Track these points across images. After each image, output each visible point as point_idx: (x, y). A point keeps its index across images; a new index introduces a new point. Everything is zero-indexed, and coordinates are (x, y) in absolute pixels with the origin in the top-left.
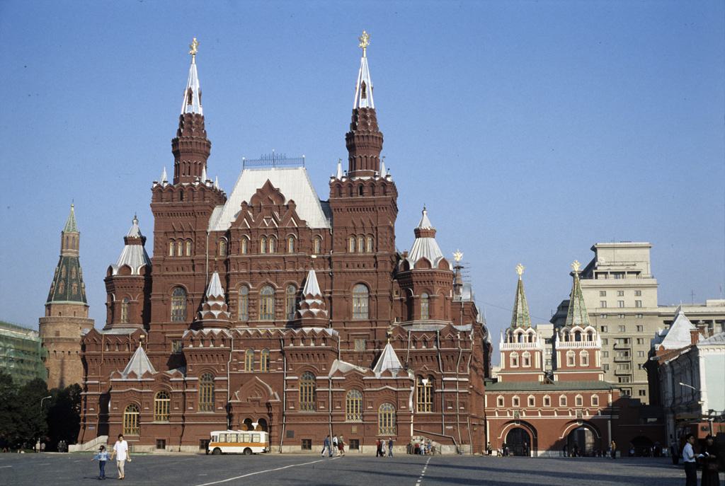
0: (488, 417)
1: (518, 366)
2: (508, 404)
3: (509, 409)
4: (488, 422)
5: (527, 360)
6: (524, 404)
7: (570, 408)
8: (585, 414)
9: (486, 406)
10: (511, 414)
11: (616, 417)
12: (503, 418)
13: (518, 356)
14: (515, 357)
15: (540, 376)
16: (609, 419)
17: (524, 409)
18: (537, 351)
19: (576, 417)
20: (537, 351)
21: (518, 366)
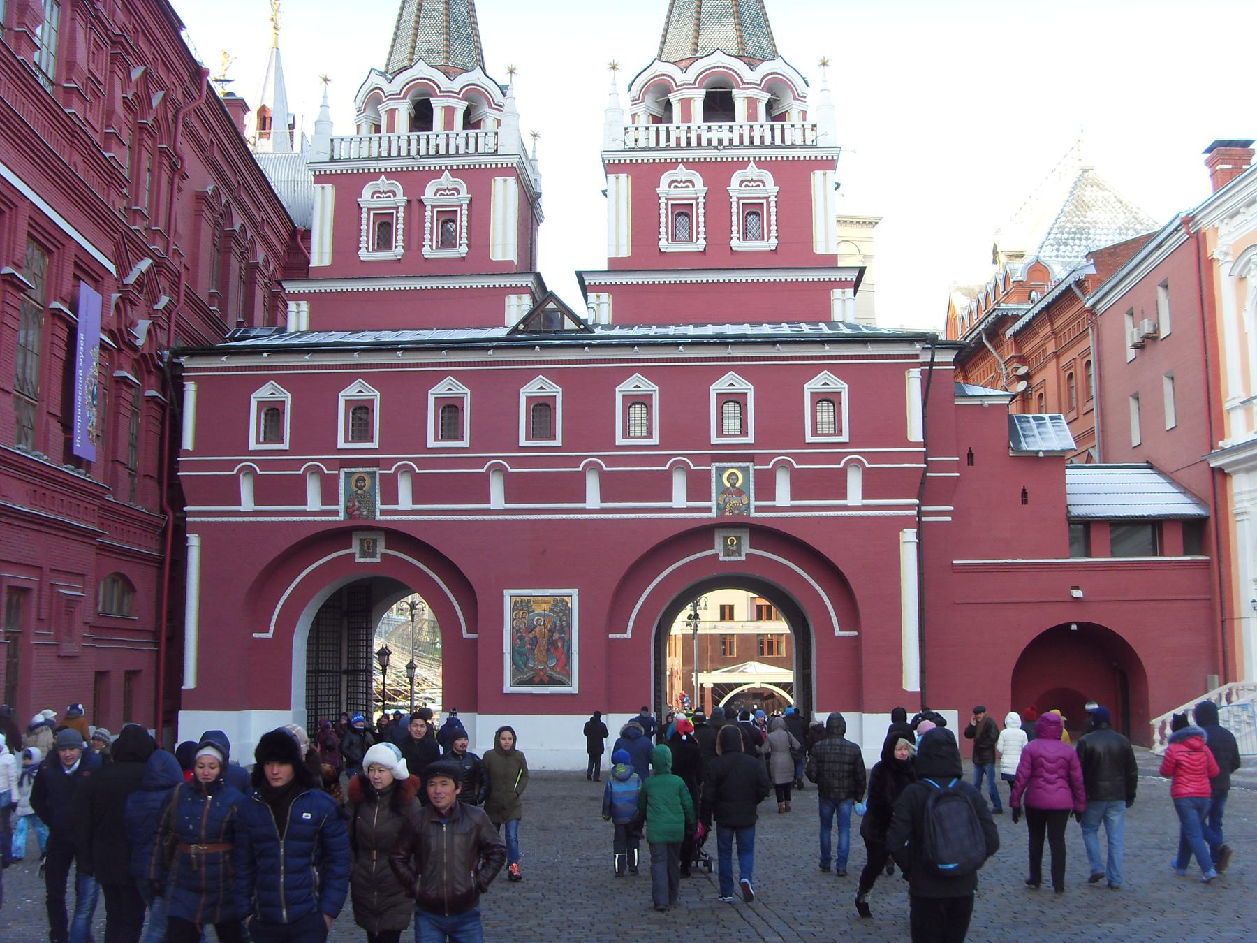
1: (398, 251)
2: (316, 433)
3: (314, 459)
4: (194, 540)
6: (404, 432)
7: (680, 455)
8: (766, 487)
9: (188, 442)
10: (329, 494)
11: (940, 513)
12: (280, 513)
13: (401, 199)
14: (385, 203)
15: (512, 300)
16: (905, 522)
17: (407, 458)
19: (711, 509)
21: (398, 251)
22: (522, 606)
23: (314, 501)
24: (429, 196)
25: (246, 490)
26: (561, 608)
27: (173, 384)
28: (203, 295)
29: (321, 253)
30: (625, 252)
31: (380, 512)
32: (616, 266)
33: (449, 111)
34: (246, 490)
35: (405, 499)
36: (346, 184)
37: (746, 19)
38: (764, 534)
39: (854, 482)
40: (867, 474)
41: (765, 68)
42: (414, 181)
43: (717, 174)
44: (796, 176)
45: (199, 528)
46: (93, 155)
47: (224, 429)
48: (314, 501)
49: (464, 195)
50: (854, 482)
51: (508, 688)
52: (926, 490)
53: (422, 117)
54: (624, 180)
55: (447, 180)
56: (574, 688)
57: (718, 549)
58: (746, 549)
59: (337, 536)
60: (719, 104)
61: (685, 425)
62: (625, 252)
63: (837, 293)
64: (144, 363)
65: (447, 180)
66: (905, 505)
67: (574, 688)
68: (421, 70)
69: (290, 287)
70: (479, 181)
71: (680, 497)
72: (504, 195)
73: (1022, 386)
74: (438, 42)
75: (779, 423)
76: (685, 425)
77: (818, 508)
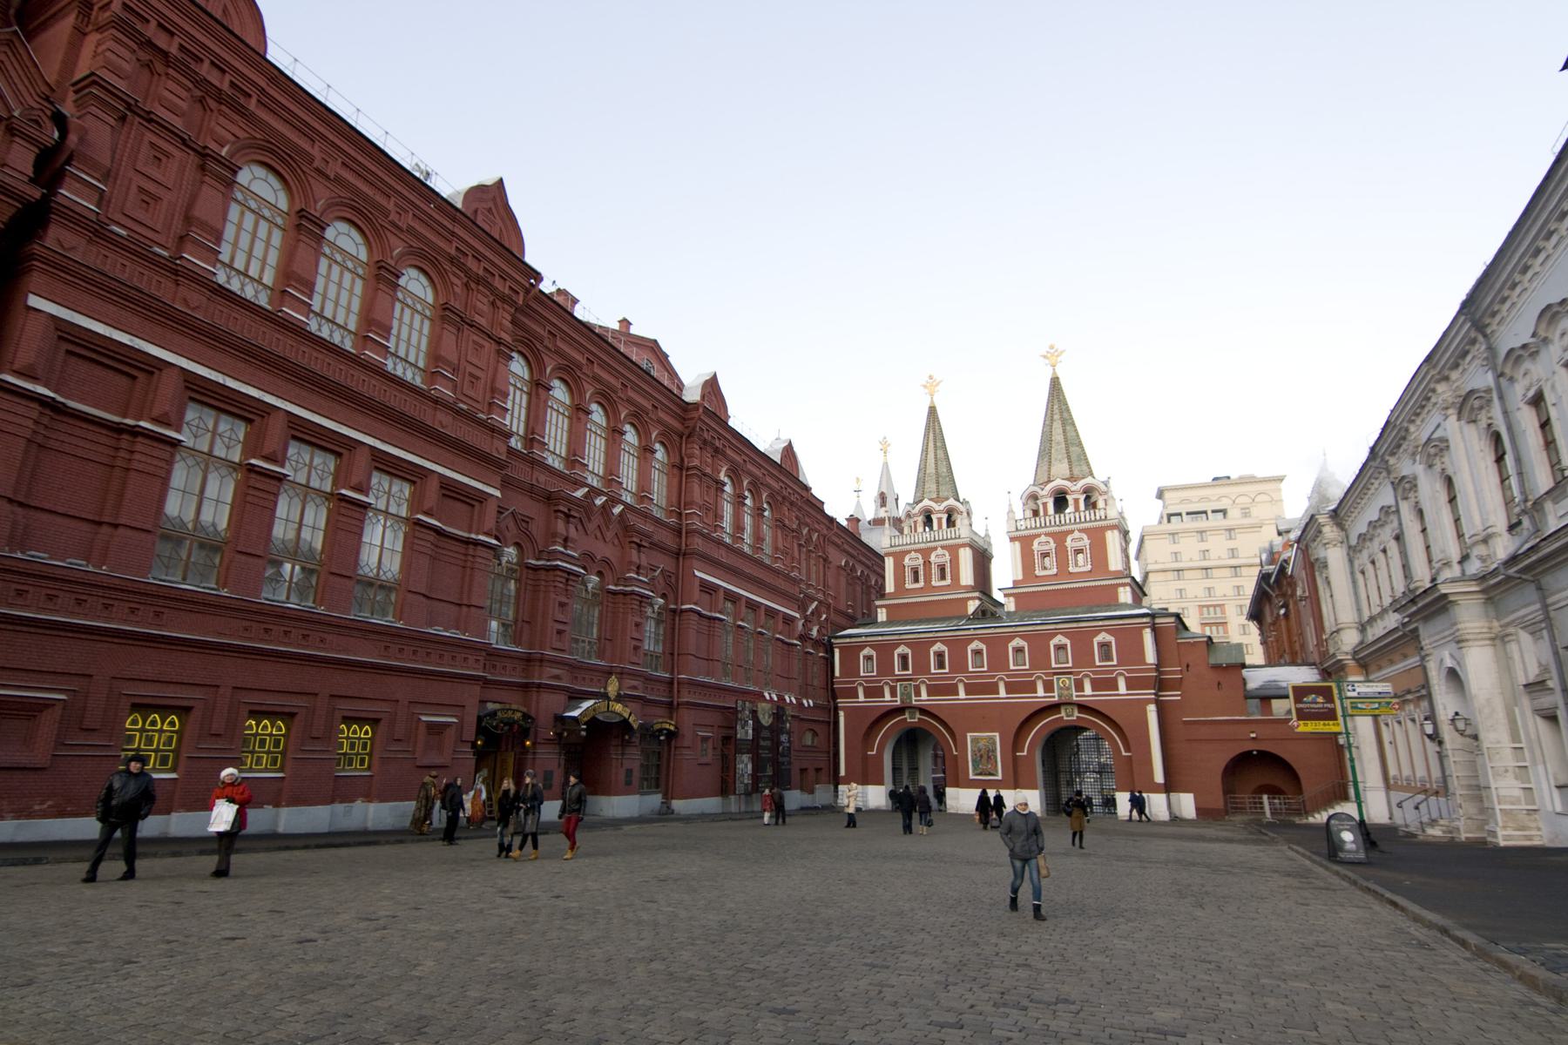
0: (842, 702)
2: (885, 667)
3: (887, 679)
4: (841, 714)
5: (942, 569)
6: (922, 667)
7: (1039, 673)
8: (1079, 686)
9: (837, 673)
10: (893, 694)
11: (1172, 696)
12: (875, 702)
13: (921, 561)
16: (1149, 701)
17: (923, 678)
18: (964, 545)
19: (1055, 697)
20: (964, 545)
22: (975, 740)
23: (888, 697)
24: (933, 558)
25: (861, 692)
26: (992, 740)
27: (830, 650)
28: (842, 607)
29: (890, 587)
30: (1020, 577)
31: (914, 701)
32: (1016, 584)
33: (940, 520)
34: (861, 692)
35: (924, 695)
36: (899, 557)
37: (1074, 457)
38: (1083, 707)
39: (1122, 684)
40: (1127, 679)
41: (1081, 483)
42: (926, 553)
43: (1060, 538)
44: (1097, 537)
45: (843, 709)
46: (787, 577)
47: (851, 667)
48: (888, 697)
49: (948, 557)
50: (1122, 684)
51: (972, 777)
52: (1161, 684)
53: (928, 521)
54: (1017, 544)
55: (940, 551)
56: (999, 777)
57: (1063, 714)
58: (1076, 714)
59: (899, 711)
60: (1061, 501)
61: (1040, 659)
62: (1020, 577)
63: (1121, 589)
64: (817, 643)
65: (940, 551)
66: (1149, 693)
67: (999, 777)
68: (926, 502)
69: (878, 603)
70: (953, 550)
71: (1040, 692)
72: (966, 557)
73: (1282, 611)
74: (934, 487)
75: (1083, 654)
76: (1040, 659)
77: (1105, 696)
